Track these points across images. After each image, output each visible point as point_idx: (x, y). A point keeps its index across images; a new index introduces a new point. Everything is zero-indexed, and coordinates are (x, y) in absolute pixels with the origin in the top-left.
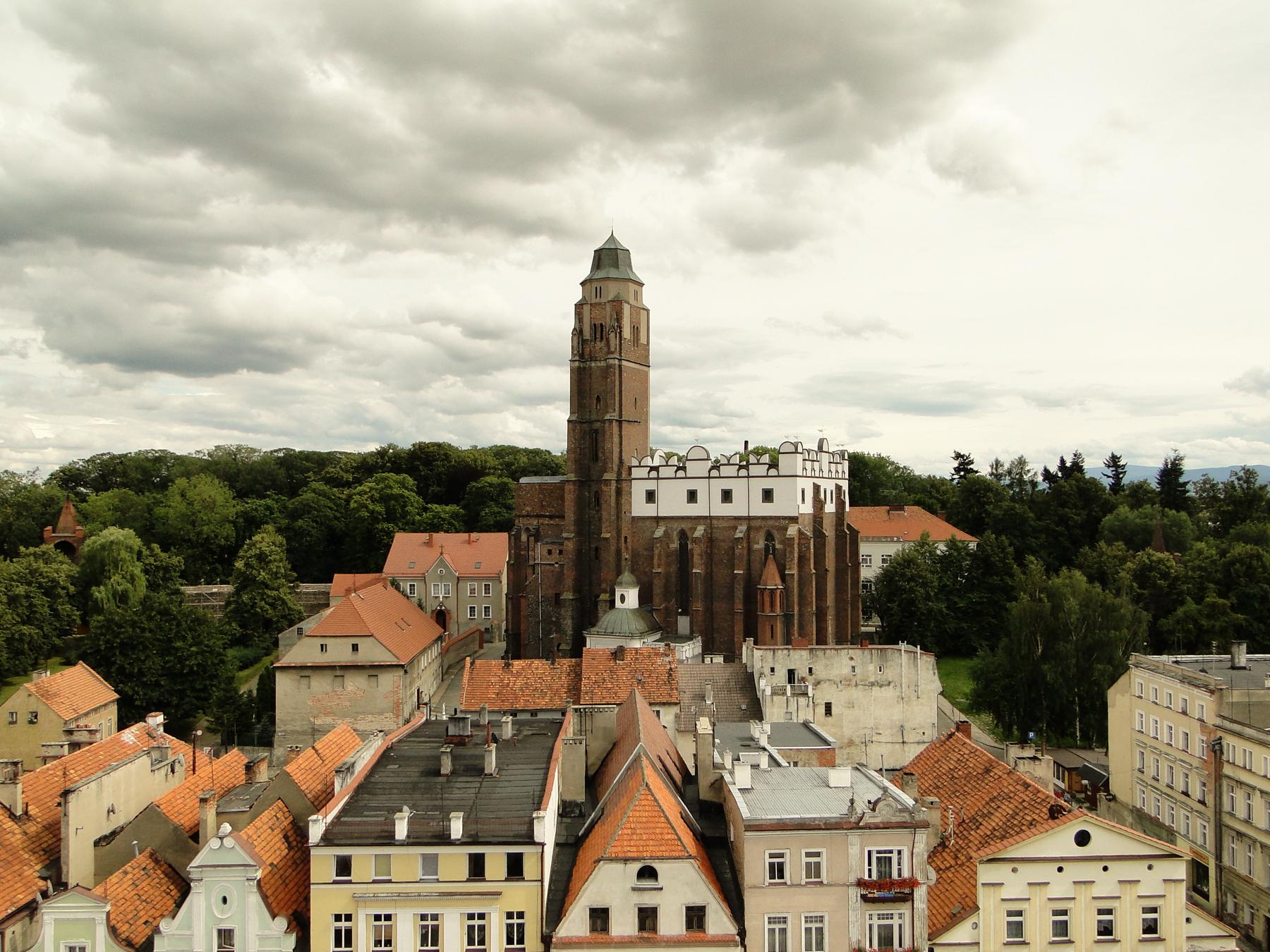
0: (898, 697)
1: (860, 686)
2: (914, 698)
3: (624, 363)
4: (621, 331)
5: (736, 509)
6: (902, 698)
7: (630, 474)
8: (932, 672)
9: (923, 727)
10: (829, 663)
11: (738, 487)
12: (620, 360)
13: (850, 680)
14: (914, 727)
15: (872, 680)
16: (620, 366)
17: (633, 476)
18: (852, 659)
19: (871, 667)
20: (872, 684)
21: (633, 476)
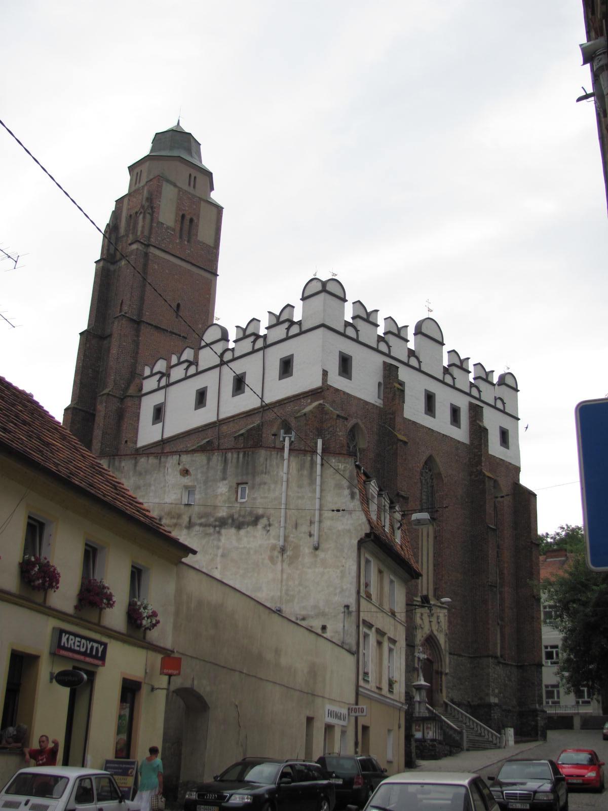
0: (273, 548)
1: (197, 528)
2: (306, 550)
3: (152, 250)
4: (153, 212)
5: (248, 401)
6: (283, 550)
7: (141, 389)
8: (347, 492)
9: (323, 614)
10: (141, 482)
11: (251, 367)
12: (148, 246)
13: (179, 516)
14: (304, 613)
15: (222, 513)
16: (146, 255)
17: (144, 391)
18: (185, 472)
19: (223, 489)
20: (222, 523)
21: (144, 391)
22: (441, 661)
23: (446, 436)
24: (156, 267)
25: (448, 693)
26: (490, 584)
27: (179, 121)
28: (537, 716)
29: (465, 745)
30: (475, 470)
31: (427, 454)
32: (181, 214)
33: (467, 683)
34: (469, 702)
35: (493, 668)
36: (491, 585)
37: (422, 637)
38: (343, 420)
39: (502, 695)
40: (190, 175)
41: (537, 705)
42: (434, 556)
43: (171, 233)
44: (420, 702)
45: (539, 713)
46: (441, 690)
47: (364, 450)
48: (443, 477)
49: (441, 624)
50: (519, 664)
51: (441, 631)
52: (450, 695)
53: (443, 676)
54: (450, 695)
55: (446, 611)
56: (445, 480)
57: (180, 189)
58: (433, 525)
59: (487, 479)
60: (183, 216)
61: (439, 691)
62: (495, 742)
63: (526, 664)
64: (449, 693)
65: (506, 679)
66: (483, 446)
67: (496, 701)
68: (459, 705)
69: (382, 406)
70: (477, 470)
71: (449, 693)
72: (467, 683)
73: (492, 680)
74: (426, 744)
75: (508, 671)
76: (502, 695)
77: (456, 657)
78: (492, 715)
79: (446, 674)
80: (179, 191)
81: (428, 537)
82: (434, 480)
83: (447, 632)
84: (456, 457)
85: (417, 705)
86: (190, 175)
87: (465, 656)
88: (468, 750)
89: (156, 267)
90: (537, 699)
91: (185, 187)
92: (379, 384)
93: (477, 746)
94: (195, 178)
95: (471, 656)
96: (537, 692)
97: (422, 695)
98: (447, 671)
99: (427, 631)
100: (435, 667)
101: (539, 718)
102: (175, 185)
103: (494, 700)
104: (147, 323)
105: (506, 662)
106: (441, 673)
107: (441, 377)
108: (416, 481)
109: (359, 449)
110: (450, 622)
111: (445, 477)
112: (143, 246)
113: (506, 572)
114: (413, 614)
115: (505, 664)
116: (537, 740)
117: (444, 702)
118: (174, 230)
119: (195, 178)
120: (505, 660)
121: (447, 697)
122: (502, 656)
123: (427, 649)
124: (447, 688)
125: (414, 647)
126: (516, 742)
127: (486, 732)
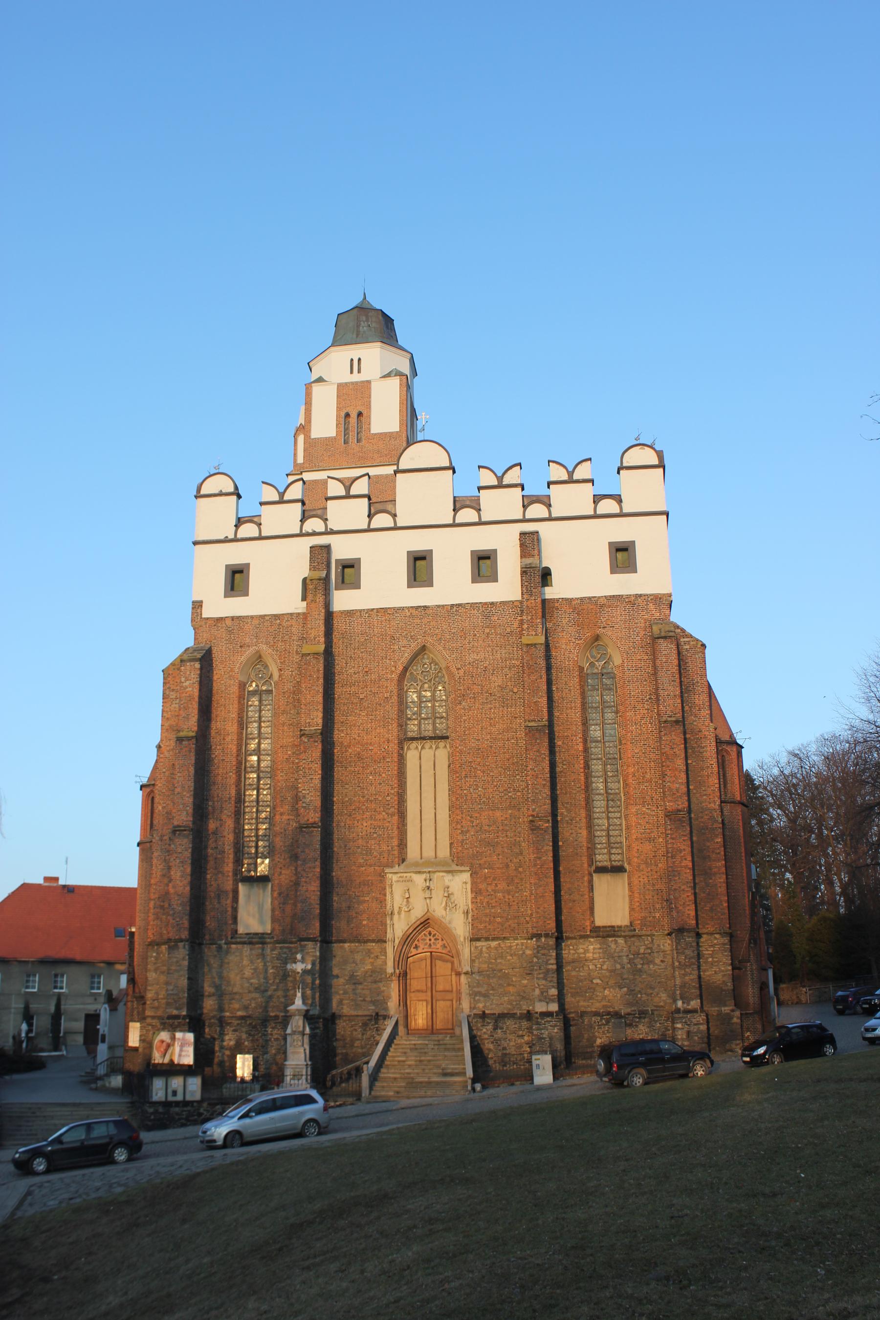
23: (460, 605)
27: (365, 294)
52: (481, 1005)
55: (466, 876)
73: (541, 976)
77: (494, 944)
79: (466, 973)
84: (487, 630)
86: (352, 360)
94: (359, 360)
99: (418, 912)
110: (476, 891)
111: (458, 669)
125: (386, 942)
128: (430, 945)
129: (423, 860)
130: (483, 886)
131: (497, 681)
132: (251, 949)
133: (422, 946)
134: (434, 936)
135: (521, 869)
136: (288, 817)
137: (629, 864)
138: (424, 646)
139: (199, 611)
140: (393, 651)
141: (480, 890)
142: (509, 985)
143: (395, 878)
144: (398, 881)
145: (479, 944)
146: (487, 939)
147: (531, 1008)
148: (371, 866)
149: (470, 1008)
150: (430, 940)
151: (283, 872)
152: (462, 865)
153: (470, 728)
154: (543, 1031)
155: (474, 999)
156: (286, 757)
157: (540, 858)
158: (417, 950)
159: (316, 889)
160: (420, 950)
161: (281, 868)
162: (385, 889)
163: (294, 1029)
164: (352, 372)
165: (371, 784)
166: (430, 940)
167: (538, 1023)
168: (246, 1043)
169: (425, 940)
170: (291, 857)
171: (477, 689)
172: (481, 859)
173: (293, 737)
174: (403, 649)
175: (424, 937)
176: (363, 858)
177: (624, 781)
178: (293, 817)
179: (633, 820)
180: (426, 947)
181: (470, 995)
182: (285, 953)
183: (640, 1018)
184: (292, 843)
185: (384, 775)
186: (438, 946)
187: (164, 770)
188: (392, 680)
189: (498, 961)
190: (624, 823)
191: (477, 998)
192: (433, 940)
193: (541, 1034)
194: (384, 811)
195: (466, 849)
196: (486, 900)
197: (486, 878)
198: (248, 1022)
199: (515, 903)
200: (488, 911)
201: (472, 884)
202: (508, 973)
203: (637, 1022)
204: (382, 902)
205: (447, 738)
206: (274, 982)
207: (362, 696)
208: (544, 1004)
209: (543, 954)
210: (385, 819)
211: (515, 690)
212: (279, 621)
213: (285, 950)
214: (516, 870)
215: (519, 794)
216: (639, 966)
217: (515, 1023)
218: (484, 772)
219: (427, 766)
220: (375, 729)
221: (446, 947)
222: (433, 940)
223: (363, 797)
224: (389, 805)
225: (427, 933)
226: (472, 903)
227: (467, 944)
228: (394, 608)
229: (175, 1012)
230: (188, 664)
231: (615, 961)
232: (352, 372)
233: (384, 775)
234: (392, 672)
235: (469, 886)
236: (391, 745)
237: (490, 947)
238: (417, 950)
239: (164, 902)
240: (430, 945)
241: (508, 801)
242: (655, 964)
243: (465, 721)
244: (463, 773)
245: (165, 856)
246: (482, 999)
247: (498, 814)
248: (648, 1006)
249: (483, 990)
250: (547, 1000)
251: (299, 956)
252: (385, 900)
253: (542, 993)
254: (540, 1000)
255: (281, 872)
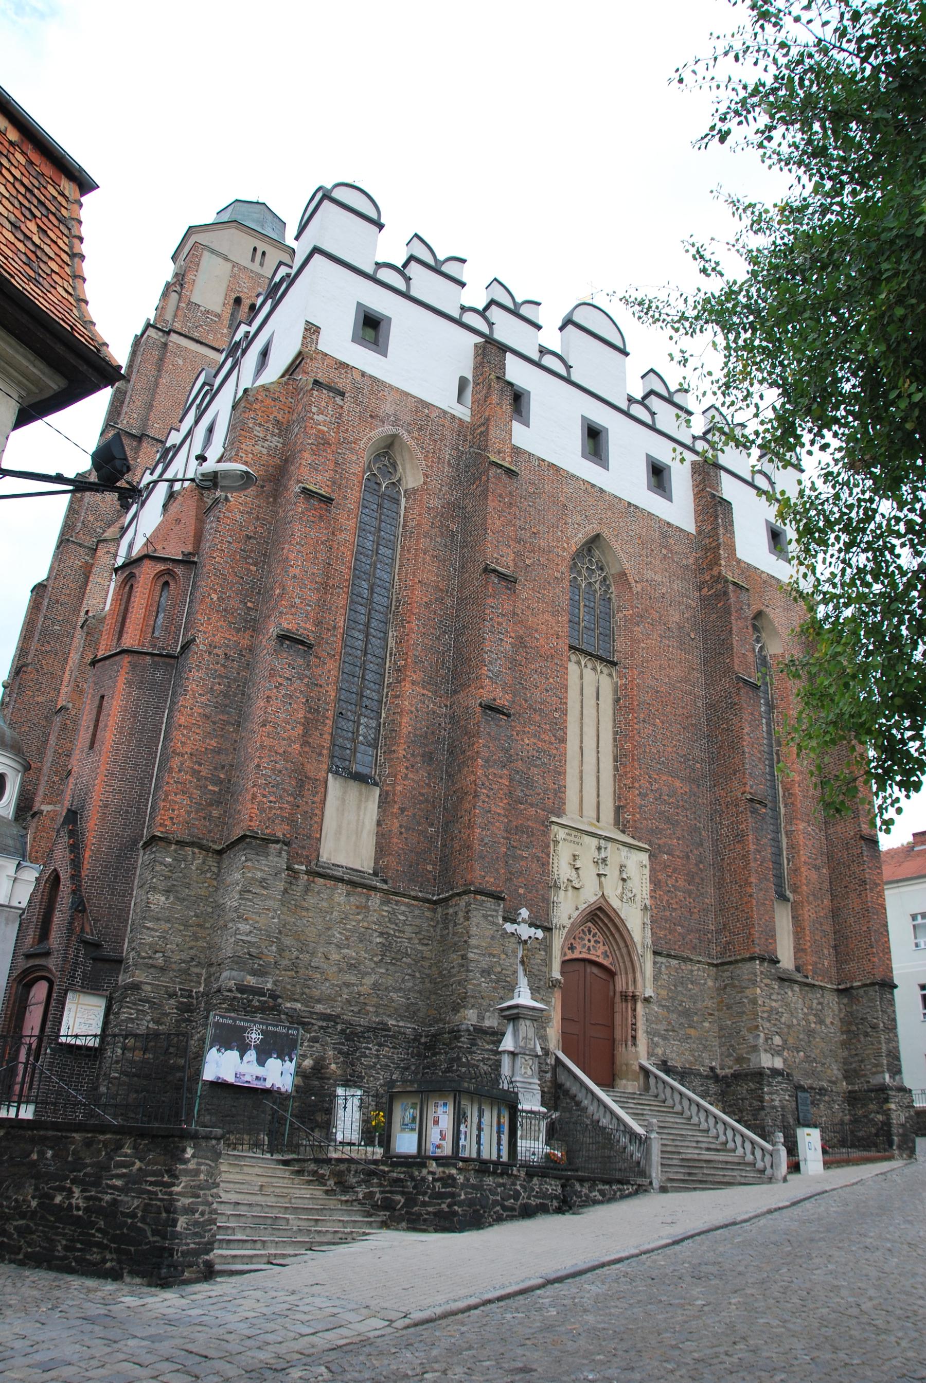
3: (174, 337)
22: (634, 973)
23: (637, 507)
24: (180, 362)
25: (652, 1046)
26: (749, 796)
28: (886, 1100)
29: (656, 1174)
30: (708, 578)
31: (590, 529)
32: (234, 296)
33: (706, 1024)
34: (712, 1069)
35: (766, 985)
36: (751, 800)
37: (577, 909)
38: (331, 394)
39: (802, 1054)
40: (255, 249)
41: (887, 1076)
42: (615, 740)
43: (212, 320)
44: (513, 1054)
45: (890, 1093)
46: (634, 1038)
47: (415, 491)
48: (631, 580)
49: (629, 884)
50: (840, 987)
51: (632, 899)
52: (659, 1051)
53: (639, 1006)
54: (659, 1051)
55: (644, 857)
56: (638, 588)
57: (235, 265)
58: (610, 675)
59: (731, 587)
60: (238, 301)
61: (629, 1043)
62: (760, 1165)
63: (855, 984)
64: (656, 1045)
65: (812, 1018)
66: (721, 531)
67: (778, 1063)
68: (683, 1075)
69: (468, 419)
70: (712, 577)
71: (656, 1045)
72: (706, 1024)
73: (765, 1015)
74: (425, 1171)
75: (815, 1001)
76: (802, 1054)
77: (674, 962)
78: (767, 1097)
79: (647, 1000)
80: (234, 266)
81: (598, 699)
82: (612, 589)
83: (648, 902)
84: (664, 551)
85: (506, 1061)
86: (255, 249)
87: (699, 962)
88: (663, 1190)
89: (180, 362)
90: (885, 1062)
91: (245, 261)
92: (463, 382)
93: (699, 1177)
94: (264, 253)
95: (715, 962)
96: (884, 1047)
97: (522, 1034)
98: (649, 992)
99: (589, 896)
100: (621, 983)
101: (893, 1106)
102: (226, 259)
103: (768, 1061)
104: (153, 439)
105: (810, 981)
106: (634, 998)
107: (624, 407)
108: (558, 575)
109: (406, 491)
110: (655, 882)
111: (636, 582)
112: (160, 334)
113: (796, 790)
114: (548, 855)
115: (807, 985)
116: (890, 1158)
117: (642, 1068)
118: (218, 316)
119: (264, 253)
120: (807, 977)
121: (650, 1055)
122: (798, 969)
123: (598, 942)
124: (650, 1033)
125: (552, 929)
126: (827, 1165)
127: (738, 1139)
128: (589, 949)
129: (584, 819)
130: (662, 876)
131: (675, 617)
132: (348, 895)
133: (579, 948)
134: (594, 936)
135: (701, 866)
136: (422, 691)
137: (794, 891)
138: (598, 536)
139: (314, 337)
140: (565, 524)
141: (659, 881)
142: (690, 1027)
143: (561, 834)
144: (564, 839)
145: (659, 959)
146: (669, 956)
147: (714, 1064)
148: (532, 805)
149: (648, 1053)
150: (589, 941)
151: (410, 775)
152: (640, 840)
153: (647, 661)
154: (774, 1097)
155: (652, 1040)
156: (425, 599)
157: (759, 852)
158: (573, 952)
159: (502, 812)
160: (576, 955)
161: (407, 768)
162: (549, 846)
163: (522, 1044)
164: (253, 260)
165: (537, 687)
166: (589, 941)
167: (770, 1085)
168: (333, 1066)
169: (583, 939)
170: (423, 756)
171: (655, 615)
172: (660, 838)
173: (437, 575)
174: (576, 526)
175: (581, 935)
176: (522, 791)
177: (786, 790)
178: (430, 694)
179: (801, 839)
180: (584, 950)
181: (647, 1032)
182: (403, 913)
183: (820, 1095)
184: (426, 733)
185: (551, 680)
186: (599, 953)
187: (229, 539)
188: (564, 559)
189: (679, 989)
190: (784, 841)
191: (656, 1039)
192: (592, 942)
193: (773, 1100)
194: (550, 731)
195: (645, 819)
196: (666, 898)
197: (666, 867)
198: (339, 1027)
199: (696, 910)
200: (668, 913)
201: (651, 871)
202: (690, 1008)
203: (818, 1100)
204: (545, 864)
205: (614, 664)
206: (381, 960)
207: (528, 562)
208: (769, 1055)
209: (766, 985)
210: (552, 744)
211: (693, 636)
212: (427, 411)
213: (403, 908)
214: (697, 865)
215: (698, 765)
216: (813, 1025)
217: (702, 1085)
218: (663, 723)
219: (589, 691)
220: (543, 613)
221: (608, 956)
222: (592, 942)
223: (526, 701)
224: (556, 724)
225: (586, 930)
226: (651, 897)
227: (649, 957)
228: (568, 472)
229: (251, 980)
230: (325, 391)
231: (792, 1014)
232: (253, 260)
233: (551, 680)
234: (564, 549)
235: (647, 871)
236: (560, 642)
237: (670, 966)
238: (573, 952)
239: (200, 765)
240: (589, 949)
241: (688, 771)
242: (826, 1026)
243: (643, 649)
244: (642, 715)
245: (213, 684)
246: (661, 1042)
247: (678, 783)
248: (822, 1080)
249: (661, 1027)
250: (773, 1052)
251: (524, 913)
252: (549, 864)
253: (767, 1039)
254: (766, 1051)
255: (406, 775)
